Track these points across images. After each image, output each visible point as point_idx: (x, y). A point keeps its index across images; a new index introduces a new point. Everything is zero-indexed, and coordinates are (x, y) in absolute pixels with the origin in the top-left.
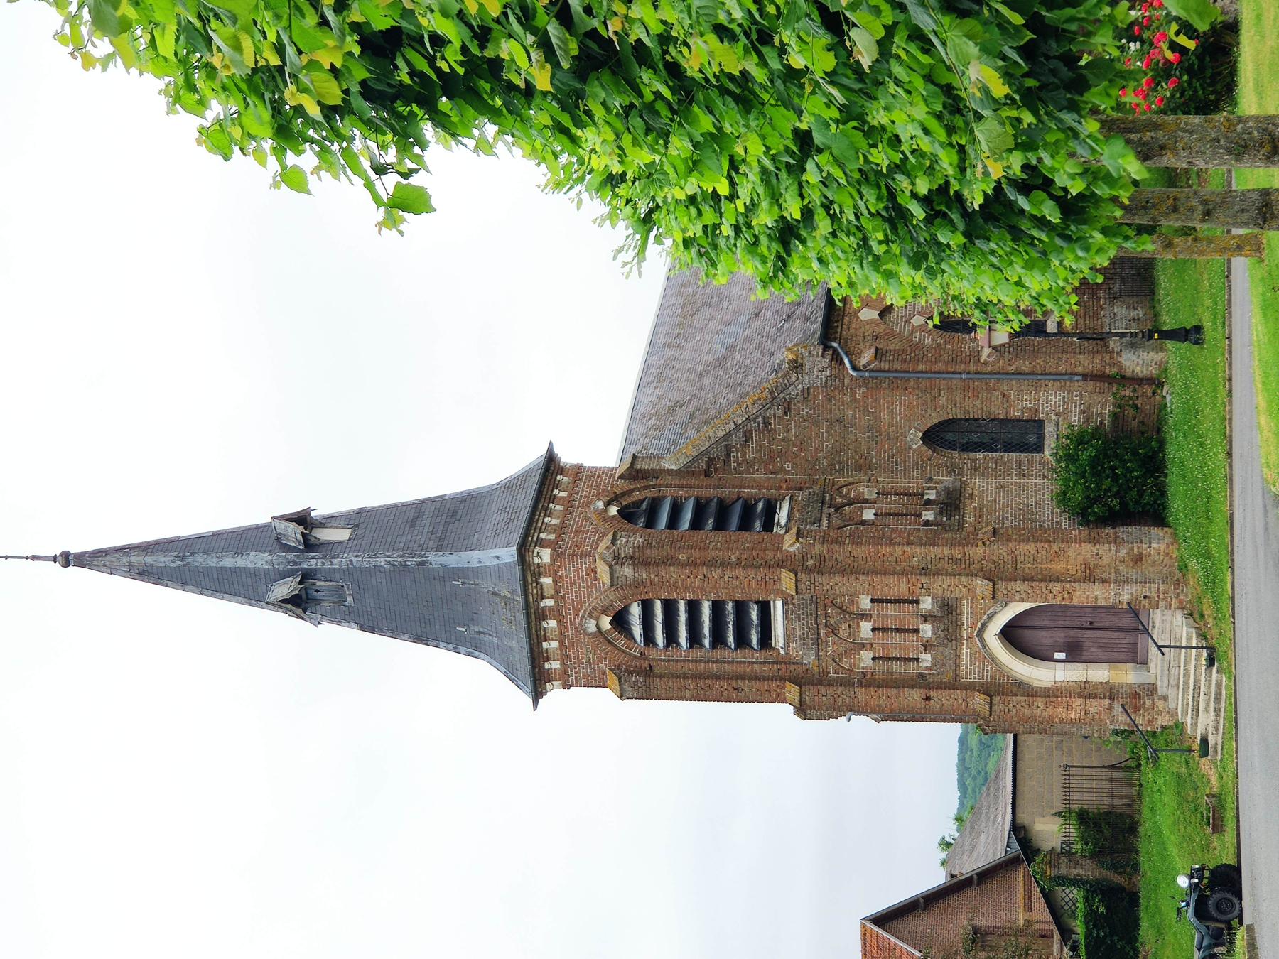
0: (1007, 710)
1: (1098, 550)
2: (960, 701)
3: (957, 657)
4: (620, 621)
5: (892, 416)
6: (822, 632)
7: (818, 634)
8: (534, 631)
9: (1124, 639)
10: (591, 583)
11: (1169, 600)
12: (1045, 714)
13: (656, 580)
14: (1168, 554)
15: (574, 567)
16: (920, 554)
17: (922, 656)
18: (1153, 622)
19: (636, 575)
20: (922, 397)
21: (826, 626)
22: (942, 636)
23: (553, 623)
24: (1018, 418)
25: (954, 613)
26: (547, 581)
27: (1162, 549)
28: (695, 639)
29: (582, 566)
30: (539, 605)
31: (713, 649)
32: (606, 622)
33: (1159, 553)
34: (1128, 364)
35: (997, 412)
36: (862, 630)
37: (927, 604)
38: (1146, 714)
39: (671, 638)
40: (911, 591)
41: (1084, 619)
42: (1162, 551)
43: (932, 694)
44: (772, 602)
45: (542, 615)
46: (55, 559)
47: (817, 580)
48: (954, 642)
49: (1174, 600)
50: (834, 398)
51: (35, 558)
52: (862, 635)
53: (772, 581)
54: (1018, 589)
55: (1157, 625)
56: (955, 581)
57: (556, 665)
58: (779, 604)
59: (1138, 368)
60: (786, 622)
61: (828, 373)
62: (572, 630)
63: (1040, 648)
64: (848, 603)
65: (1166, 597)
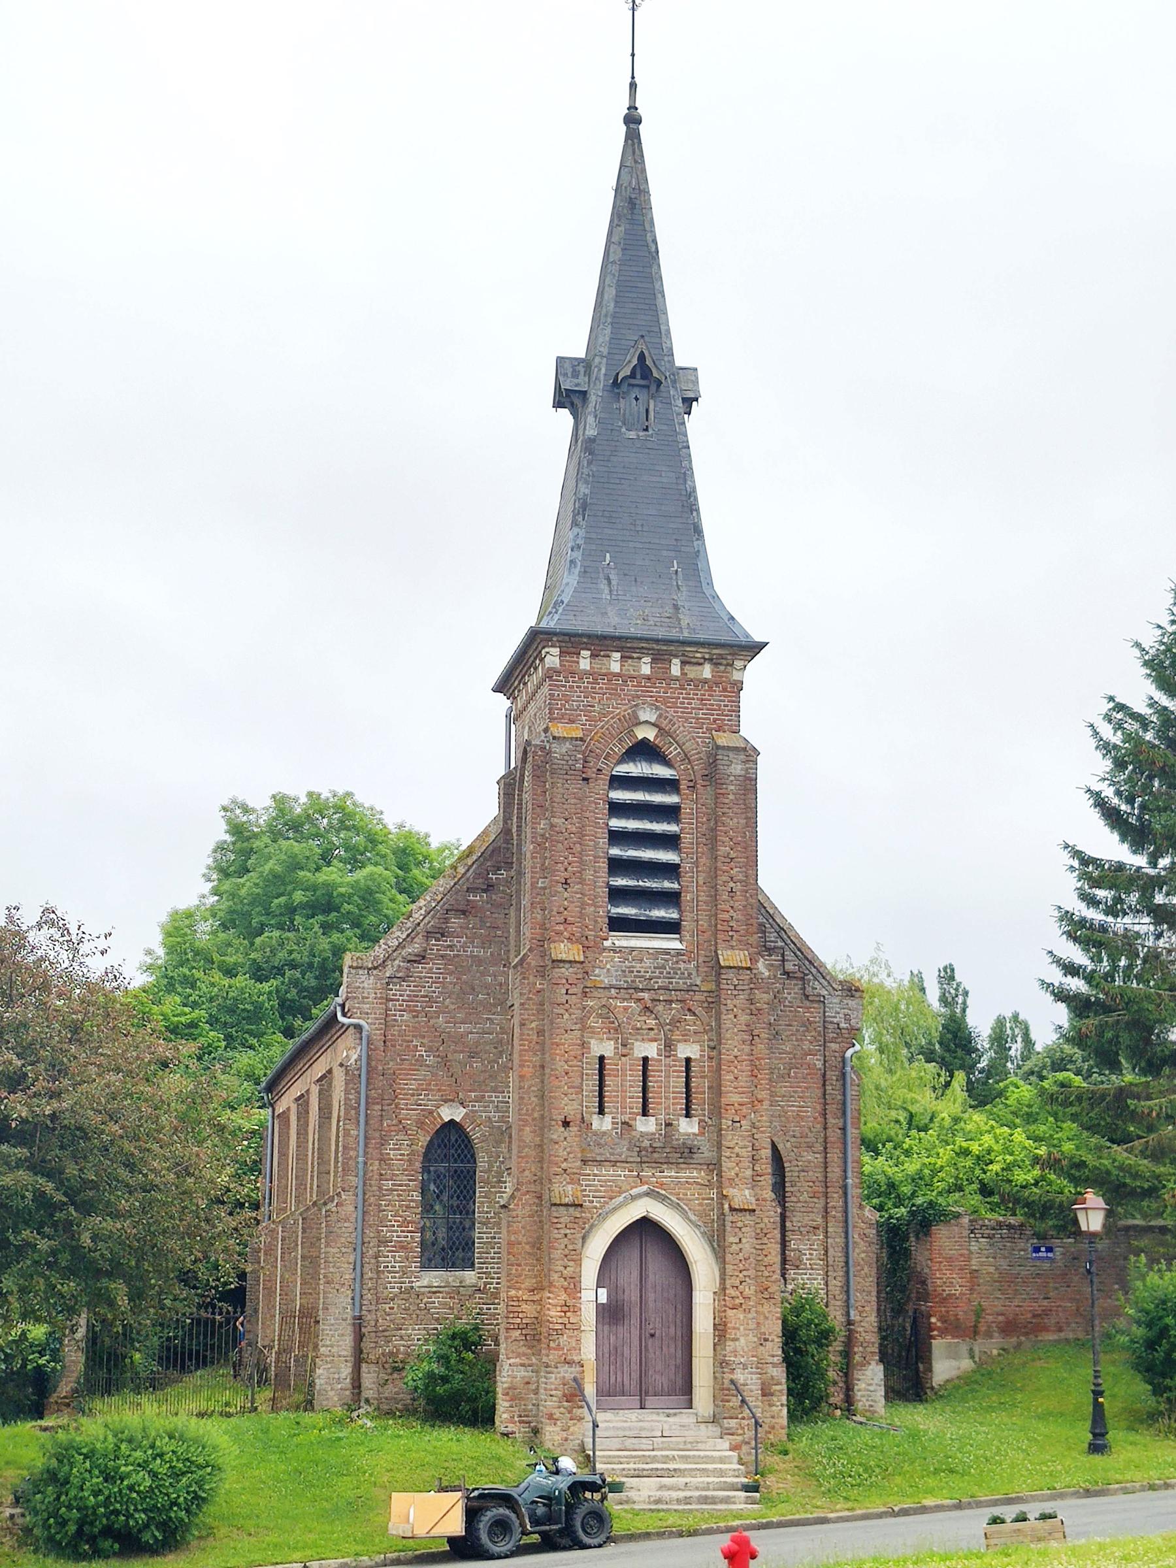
0: (559, 1226)
1: (772, 1341)
2: (564, 1165)
3: (614, 1163)
4: (644, 750)
5: (784, 1096)
6: (646, 995)
7: (642, 990)
8: (644, 645)
9: (630, 1380)
10: (703, 723)
11: (740, 1432)
12: (555, 1276)
13: (726, 801)
14: (773, 1428)
15: (725, 706)
16: (759, 1121)
17: (608, 1119)
18: (675, 1414)
19: (732, 778)
20: (811, 1132)
21: (653, 1000)
22: (643, 1145)
23: (646, 670)
24: (788, 1244)
25: (681, 1160)
26: (707, 672)
27: (780, 1420)
28: (617, 837)
29: (727, 716)
30: (676, 656)
31: (609, 859)
32: (646, 733)
33: (773, 1417)
34: (869, 1373)
35: (794, 1219)
36: (647, 1045)
37: (687, 1127)
38: (562, 1410)
39: (617, 809)
40: (728, 1107)
41: (658, 1325)
42: (777, 1421)
43: (573, 1129)
44: (678, 936)
45: (661, 659)
46: (633, 107)
47: (741, 992)
48: (639, 1160)
49: (740, 1438)
50: (808, 1030)
51: (633, 86)
52: (637, 1044)
53: (729, 938)
54: (744, 1240)
55: (671, 1419)
56: (746, 1163)
57: (585, 664)
58: (677, 945)
59: (864, 1385)
60: (651, 951)
61: (842, 1025)
62: (635, 691)
63: (613, 1267)
64: (685, 1030)
65: (743, 1428)
